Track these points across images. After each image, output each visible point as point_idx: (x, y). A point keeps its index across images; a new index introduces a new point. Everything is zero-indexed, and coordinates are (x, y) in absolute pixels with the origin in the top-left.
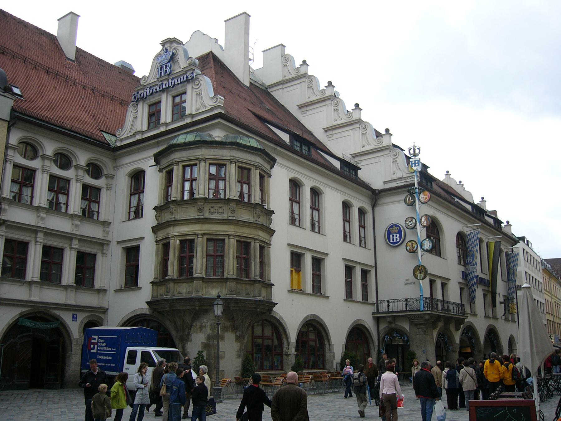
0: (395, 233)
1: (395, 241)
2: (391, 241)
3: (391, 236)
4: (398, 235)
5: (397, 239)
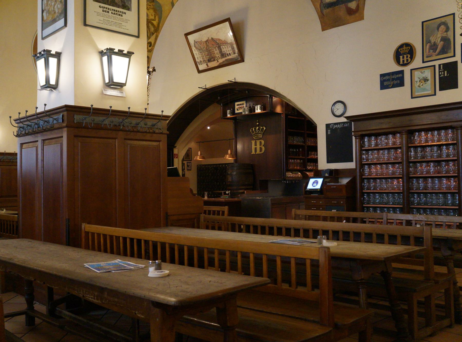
0: (405, 53)
1: (405, 62)
2: (401, 63)
3: (401, 57)
4: (409, 56)
5: (407, 60)
